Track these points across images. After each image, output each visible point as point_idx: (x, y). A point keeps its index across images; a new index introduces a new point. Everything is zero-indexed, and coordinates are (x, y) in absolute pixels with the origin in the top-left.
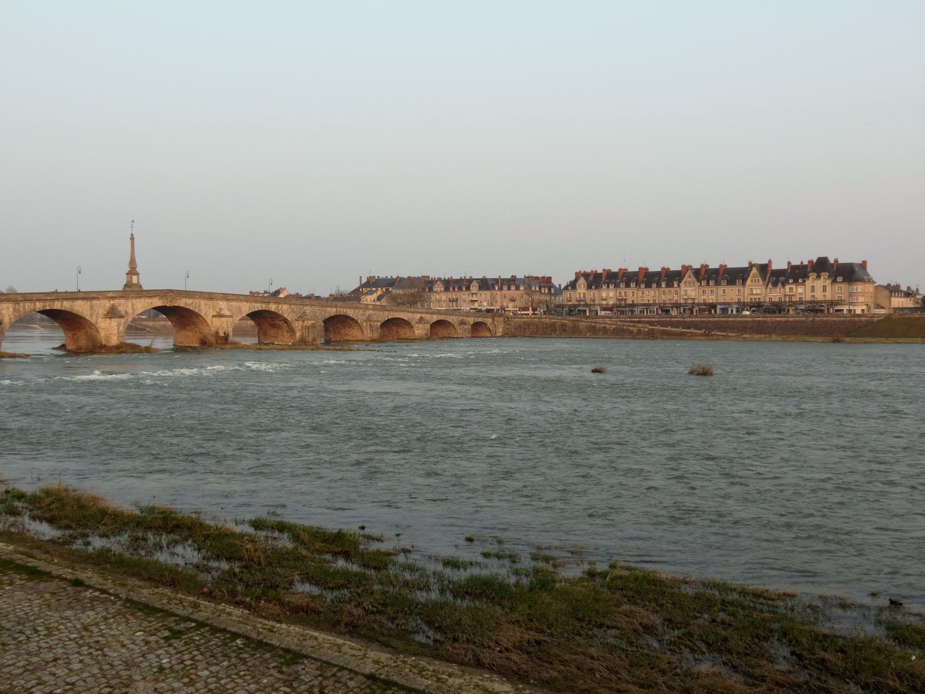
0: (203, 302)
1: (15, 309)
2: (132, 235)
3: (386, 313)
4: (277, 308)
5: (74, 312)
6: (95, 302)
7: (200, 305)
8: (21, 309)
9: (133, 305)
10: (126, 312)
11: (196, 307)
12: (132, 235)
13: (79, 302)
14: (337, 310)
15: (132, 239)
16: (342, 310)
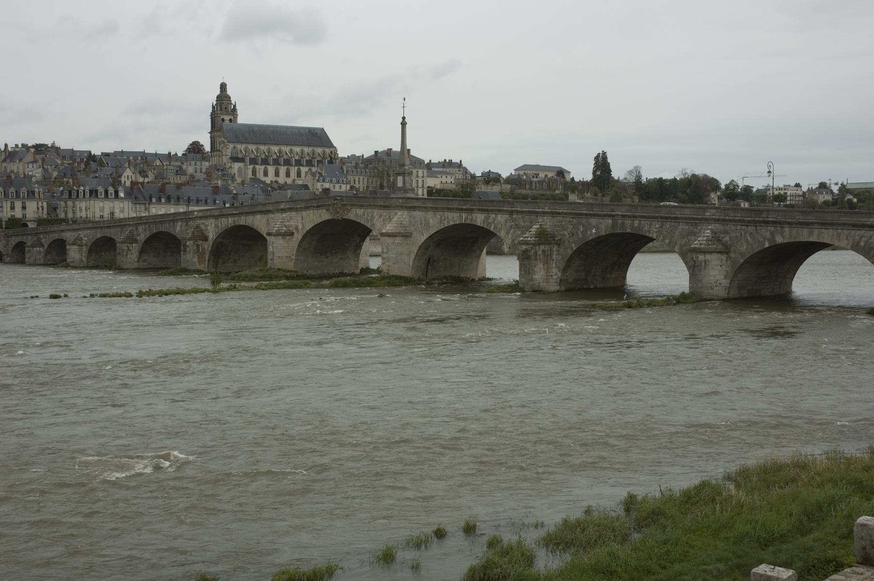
0: (376, 212)
1: (216, 226)
2: (404, 118)
3: (766, 232)
4: (486, 219)
5: (255, 227)
6: (271, 216)
7: (373, 217)
8: (219, 225)
9: (302, 219)
10: (297, 228)
11: (368, 221)
12: (404, 118)
13: (258, 217)
14: (614, 226)
15: (404, 124)
16: (628, 222)
